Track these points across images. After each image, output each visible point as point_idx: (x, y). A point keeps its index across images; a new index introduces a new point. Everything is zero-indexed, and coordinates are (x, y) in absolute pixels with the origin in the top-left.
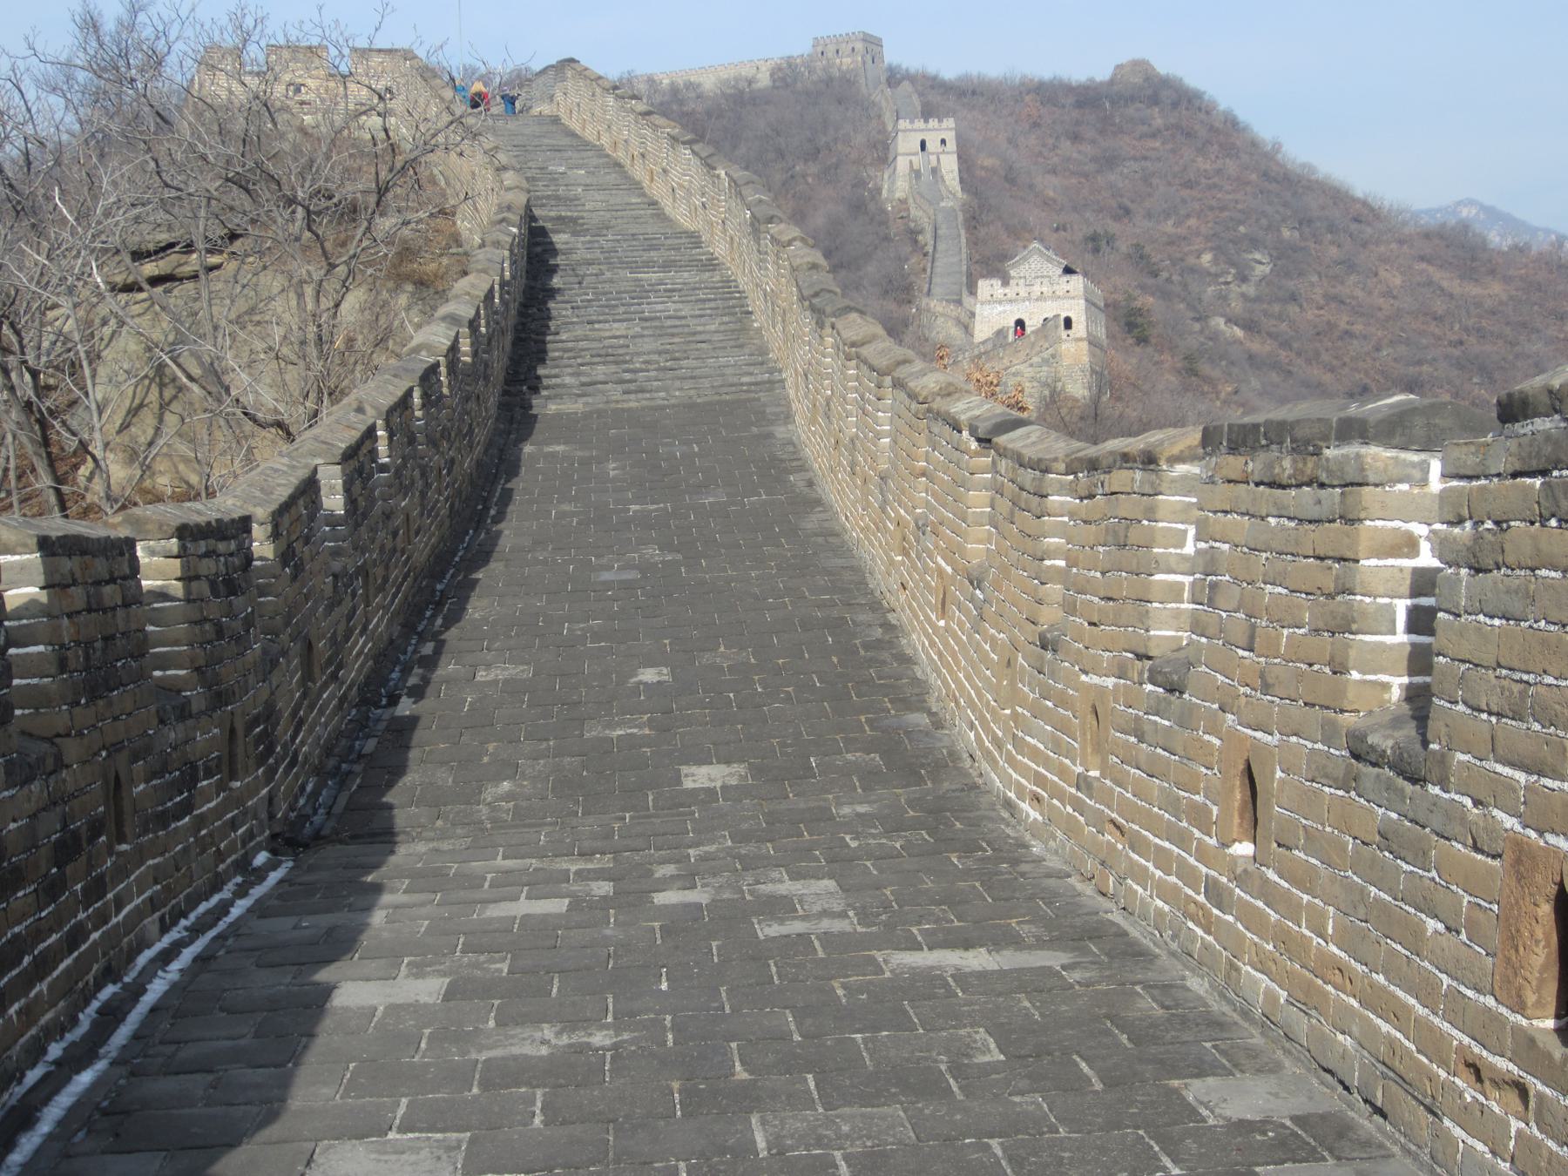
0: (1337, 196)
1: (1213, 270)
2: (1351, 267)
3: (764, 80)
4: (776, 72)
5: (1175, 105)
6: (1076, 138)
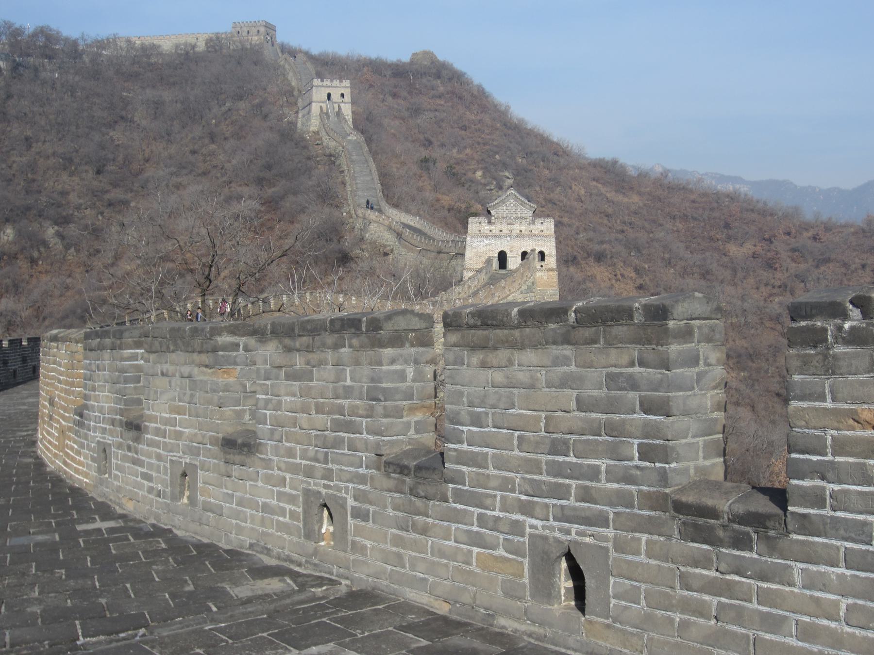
0: (544, 140)
1: (483, 181)
2: (558, 183)
3: (201, 47)
4: (208, 41)
5: (450, 79)
6: (395, 96)
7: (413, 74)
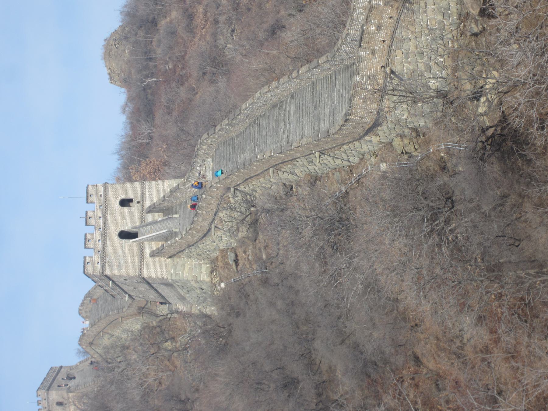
7: (147, 77)
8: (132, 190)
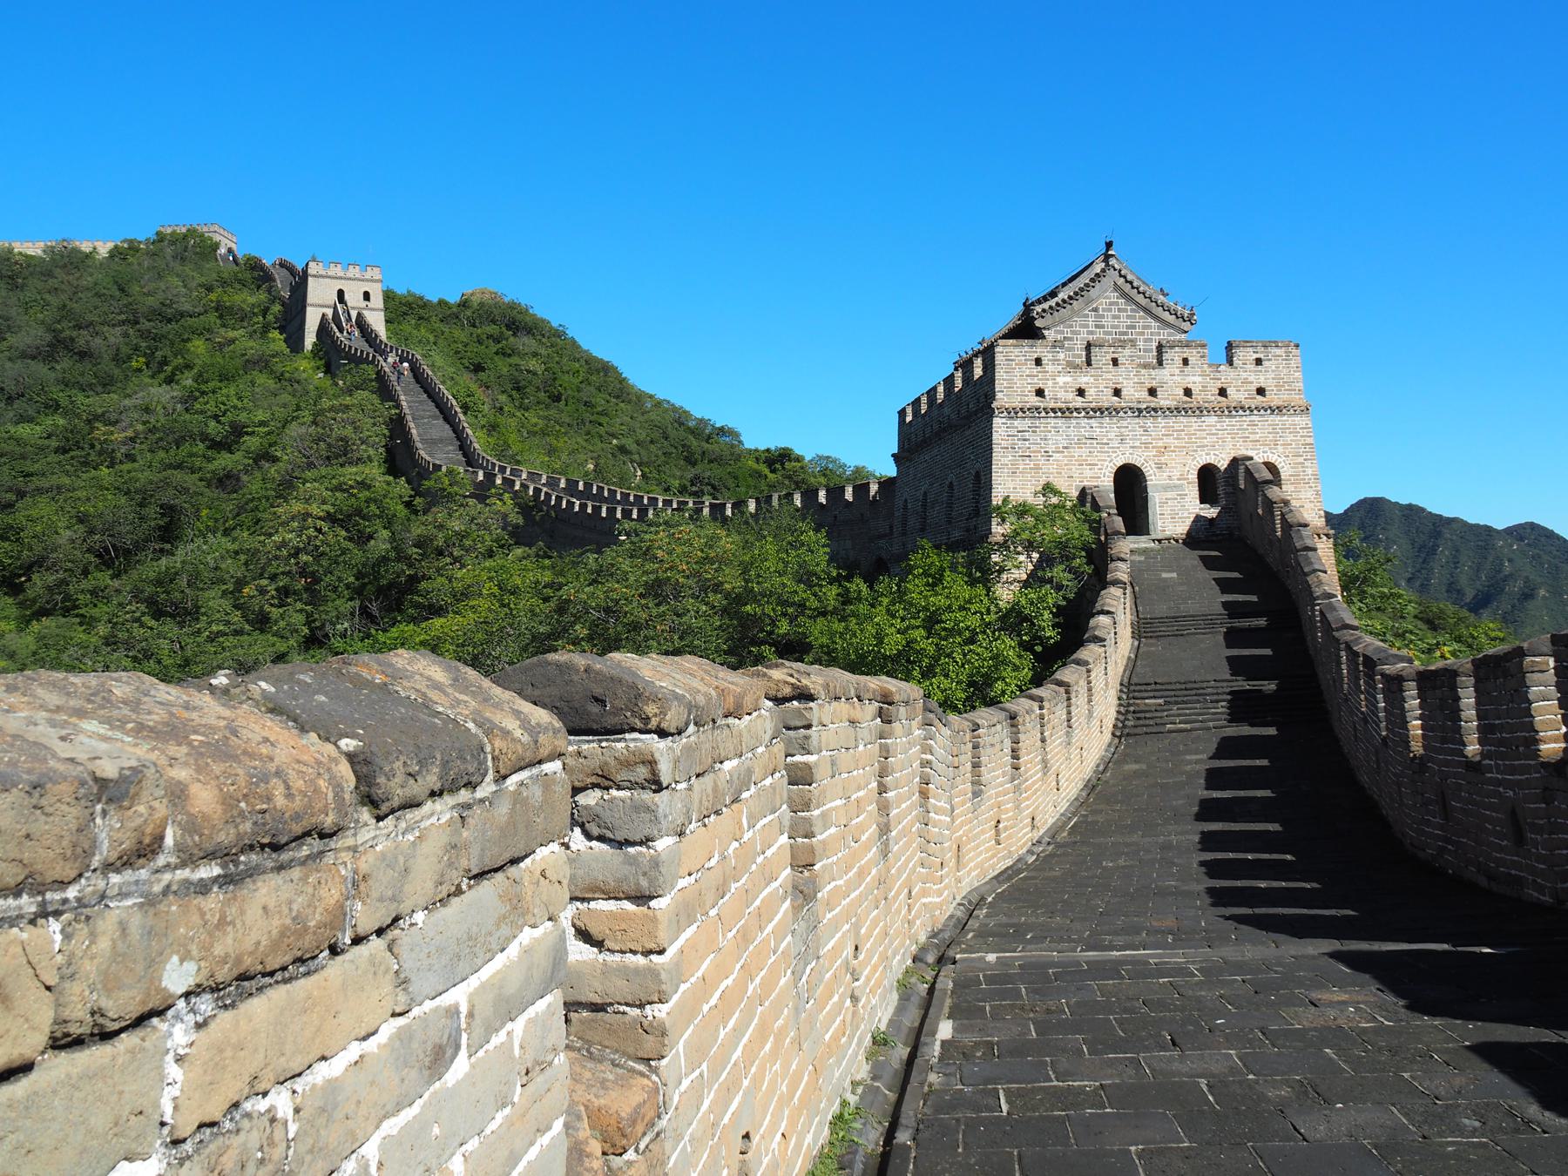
8: (377, 300)
